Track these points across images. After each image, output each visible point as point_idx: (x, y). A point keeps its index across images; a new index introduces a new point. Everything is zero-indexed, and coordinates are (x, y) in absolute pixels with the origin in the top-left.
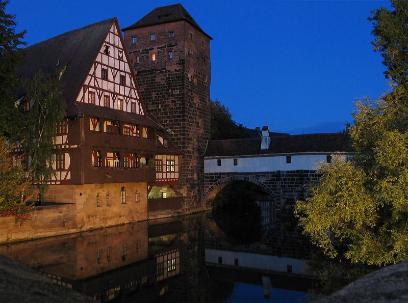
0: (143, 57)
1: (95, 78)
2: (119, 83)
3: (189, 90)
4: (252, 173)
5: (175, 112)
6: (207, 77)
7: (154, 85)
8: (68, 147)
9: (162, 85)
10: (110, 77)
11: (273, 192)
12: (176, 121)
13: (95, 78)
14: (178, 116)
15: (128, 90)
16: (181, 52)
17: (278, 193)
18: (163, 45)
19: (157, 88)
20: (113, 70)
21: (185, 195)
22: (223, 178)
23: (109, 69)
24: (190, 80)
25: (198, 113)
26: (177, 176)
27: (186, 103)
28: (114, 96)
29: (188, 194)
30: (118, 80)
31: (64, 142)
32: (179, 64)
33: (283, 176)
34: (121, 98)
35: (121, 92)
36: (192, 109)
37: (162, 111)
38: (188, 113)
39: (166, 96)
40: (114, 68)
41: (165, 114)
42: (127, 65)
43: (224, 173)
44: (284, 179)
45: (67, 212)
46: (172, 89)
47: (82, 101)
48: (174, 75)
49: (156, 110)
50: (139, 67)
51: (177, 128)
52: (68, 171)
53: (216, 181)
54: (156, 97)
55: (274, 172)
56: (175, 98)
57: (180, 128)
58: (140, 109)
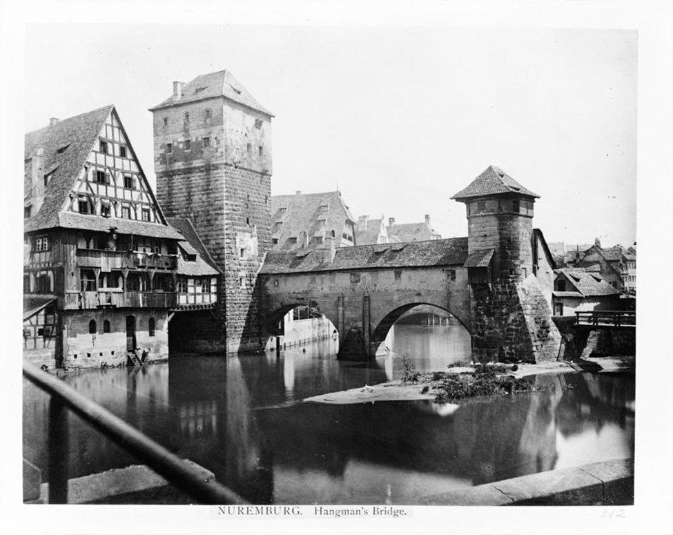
26: (214, 299)
35: (128, 197)
42: (133, 163)
58: (156, 217)
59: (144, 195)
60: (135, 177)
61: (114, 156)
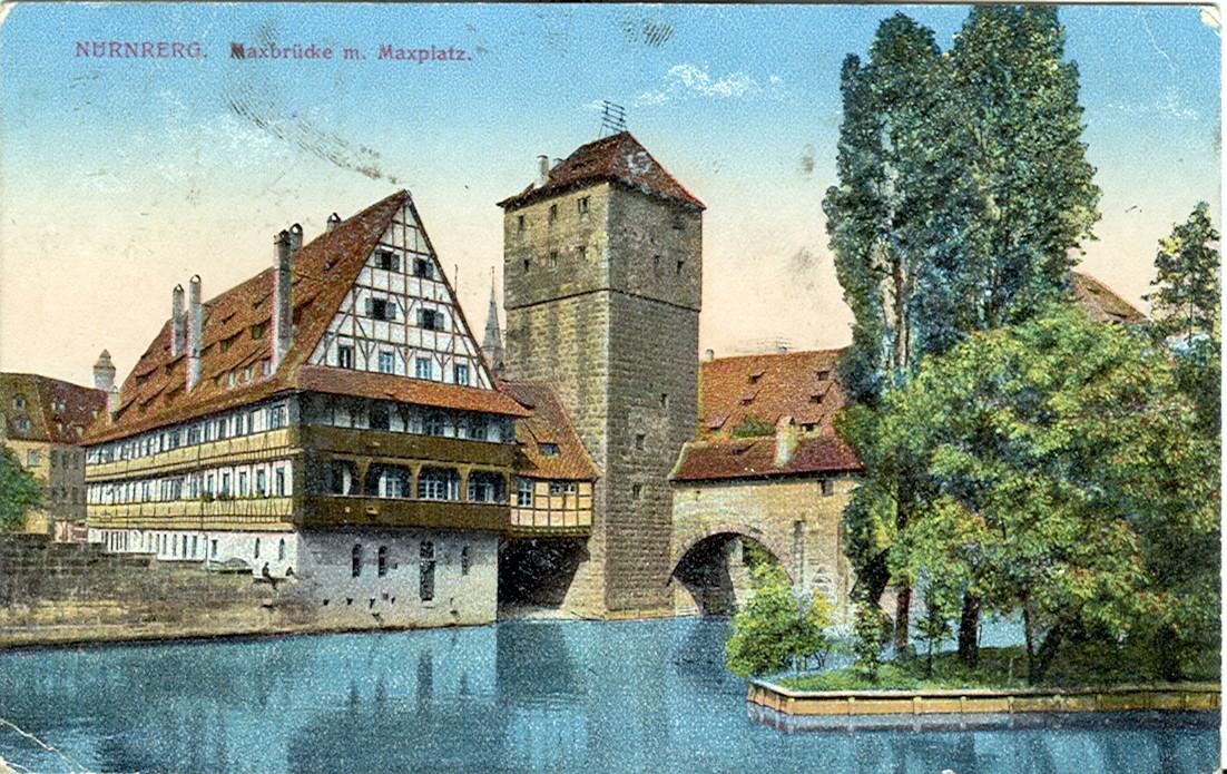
1: (355, 317)
13: (355, 317)
28: (406, 354)
30: (413, 319)
34: (427, 355)
40: (406, 296)
42: (442, 290)
60: (442, 309)
61: (406, 274)
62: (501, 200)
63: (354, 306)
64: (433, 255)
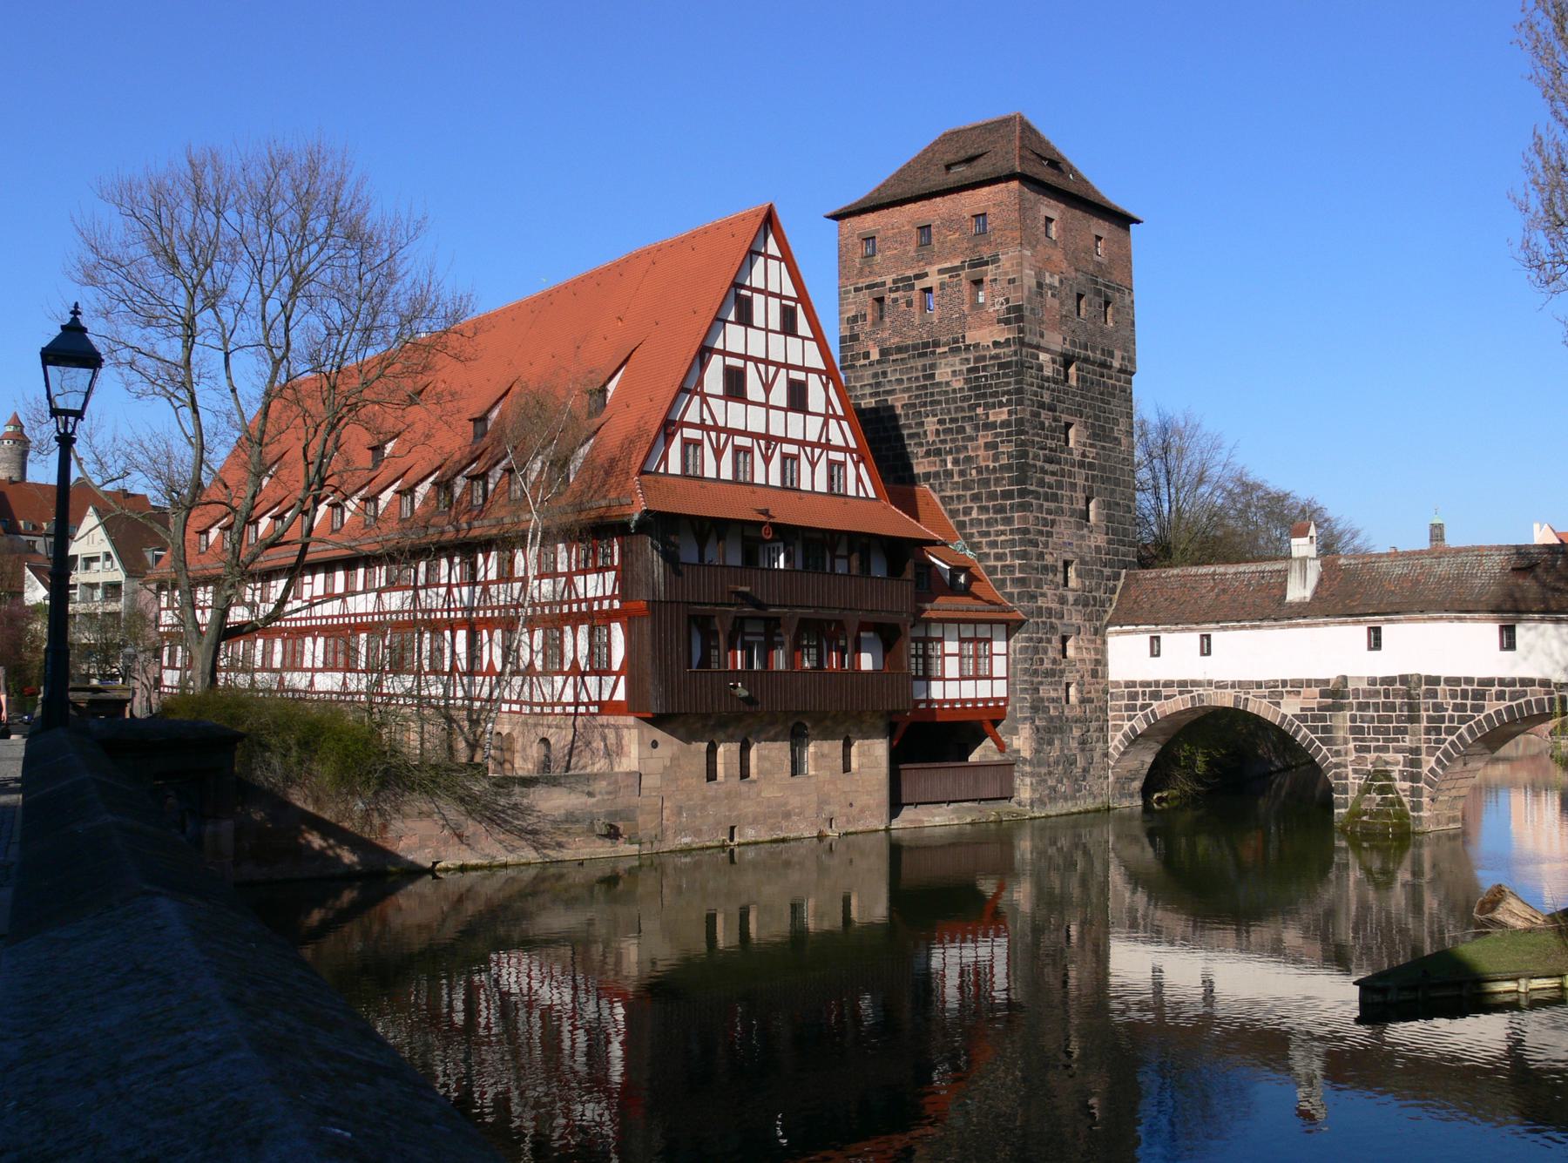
0: (895, 300)
2: (784, 404)
3: (1042, 405)
4: (1259, 685)
5: (998, 481)
6: (1118, 354)
7: (932, 394)
8: (617, 605)
9: (954, 391)
10: (754, 390)
11: (1324, 748)
12: (1000, 509)
14: (1007, 495)
15: (815, 424)
16: (1011, 281)
17: (1338, 754)
18: (957, 263)
19: (939, 402)
20: (762, 367)
21: (1026, 753)
22: (1168, 697)
23: (750, 365)
24: (1048, 372)
25: (1080, 482)
27: (1032, 451)
29: (1037, 751)
30: (780, 395)
31: (608, 593)
32: (1007, 322)
33: (1356, 692)
34: (791, 449)
36: (1049, 467)
37: (956, 479)
38: (1041, 483)
39: (968, 429)
40: (767, 362)
41: (966, 486)
42: (812, 347)
43: (1169, 684)
44: (1363, 707)
45: (609, 793)
46: (986, 406)
47: (661, 470)
48: (992, 358)
49: (937, 475)
50: (886, 335)
51: (1003, 533)
52: (618, 674)
53: (1143, 707)
54: (938, 432)
55: (1327, 682)
56: (997, 435)
57: (1012, 531)
58: (859, 479)
59: (832, 422)
61: (767, 330)
62: (828, 213)
63: (701, 382)
64: (803, 297)
